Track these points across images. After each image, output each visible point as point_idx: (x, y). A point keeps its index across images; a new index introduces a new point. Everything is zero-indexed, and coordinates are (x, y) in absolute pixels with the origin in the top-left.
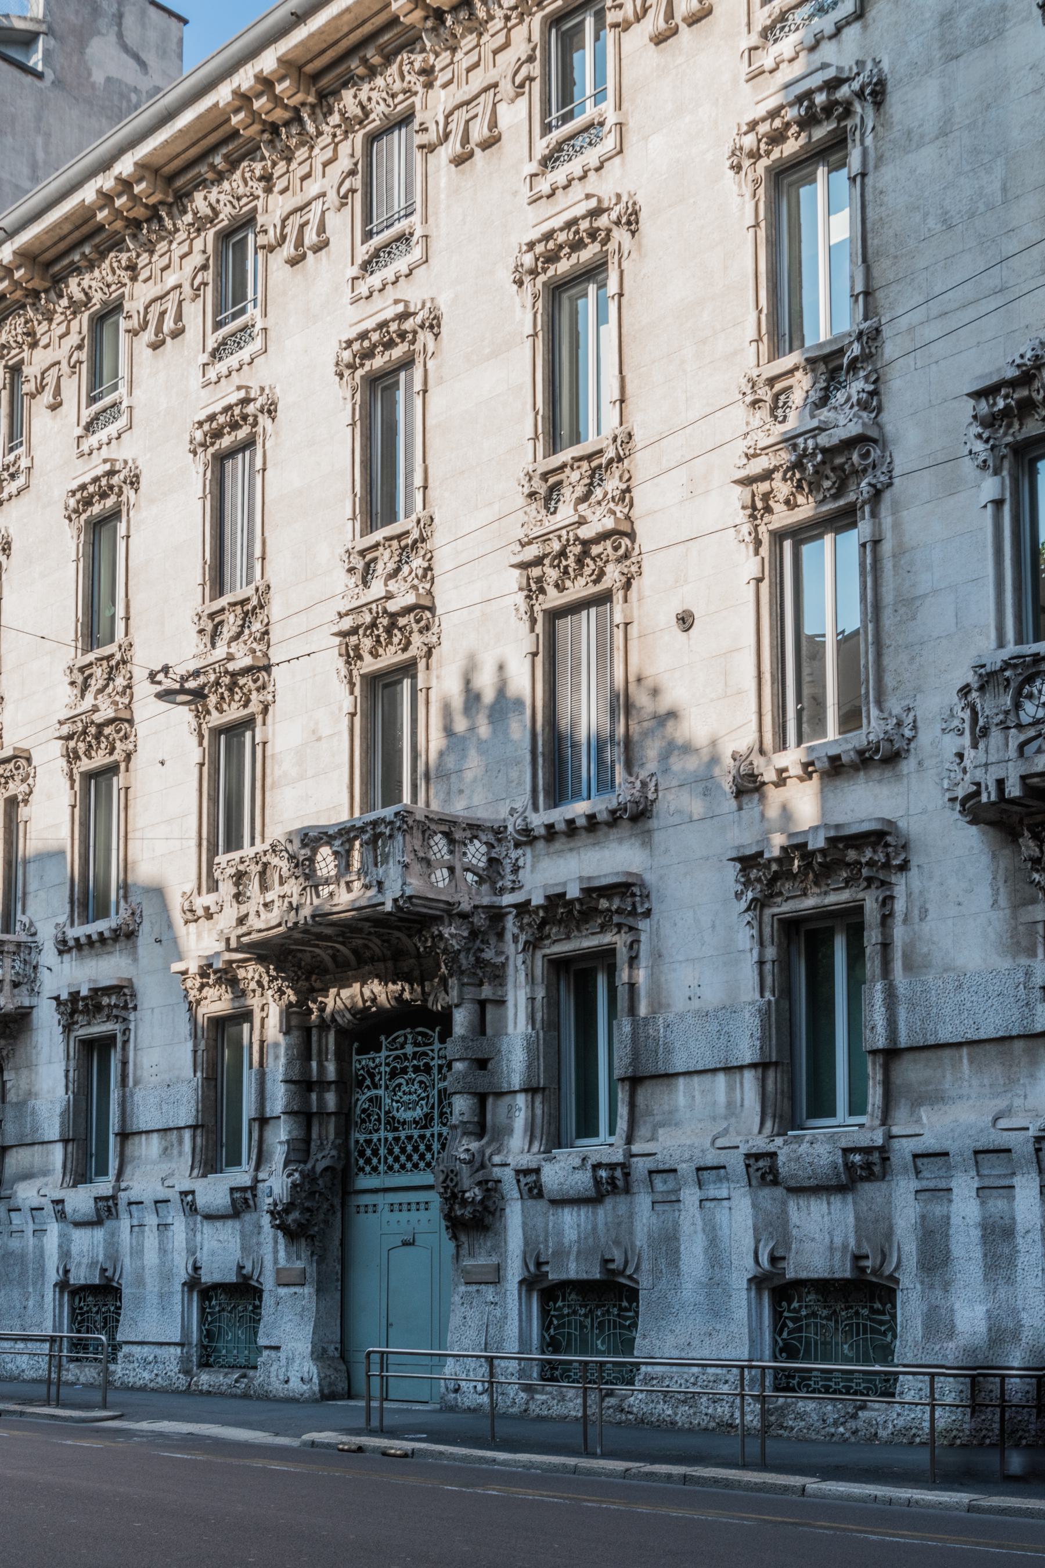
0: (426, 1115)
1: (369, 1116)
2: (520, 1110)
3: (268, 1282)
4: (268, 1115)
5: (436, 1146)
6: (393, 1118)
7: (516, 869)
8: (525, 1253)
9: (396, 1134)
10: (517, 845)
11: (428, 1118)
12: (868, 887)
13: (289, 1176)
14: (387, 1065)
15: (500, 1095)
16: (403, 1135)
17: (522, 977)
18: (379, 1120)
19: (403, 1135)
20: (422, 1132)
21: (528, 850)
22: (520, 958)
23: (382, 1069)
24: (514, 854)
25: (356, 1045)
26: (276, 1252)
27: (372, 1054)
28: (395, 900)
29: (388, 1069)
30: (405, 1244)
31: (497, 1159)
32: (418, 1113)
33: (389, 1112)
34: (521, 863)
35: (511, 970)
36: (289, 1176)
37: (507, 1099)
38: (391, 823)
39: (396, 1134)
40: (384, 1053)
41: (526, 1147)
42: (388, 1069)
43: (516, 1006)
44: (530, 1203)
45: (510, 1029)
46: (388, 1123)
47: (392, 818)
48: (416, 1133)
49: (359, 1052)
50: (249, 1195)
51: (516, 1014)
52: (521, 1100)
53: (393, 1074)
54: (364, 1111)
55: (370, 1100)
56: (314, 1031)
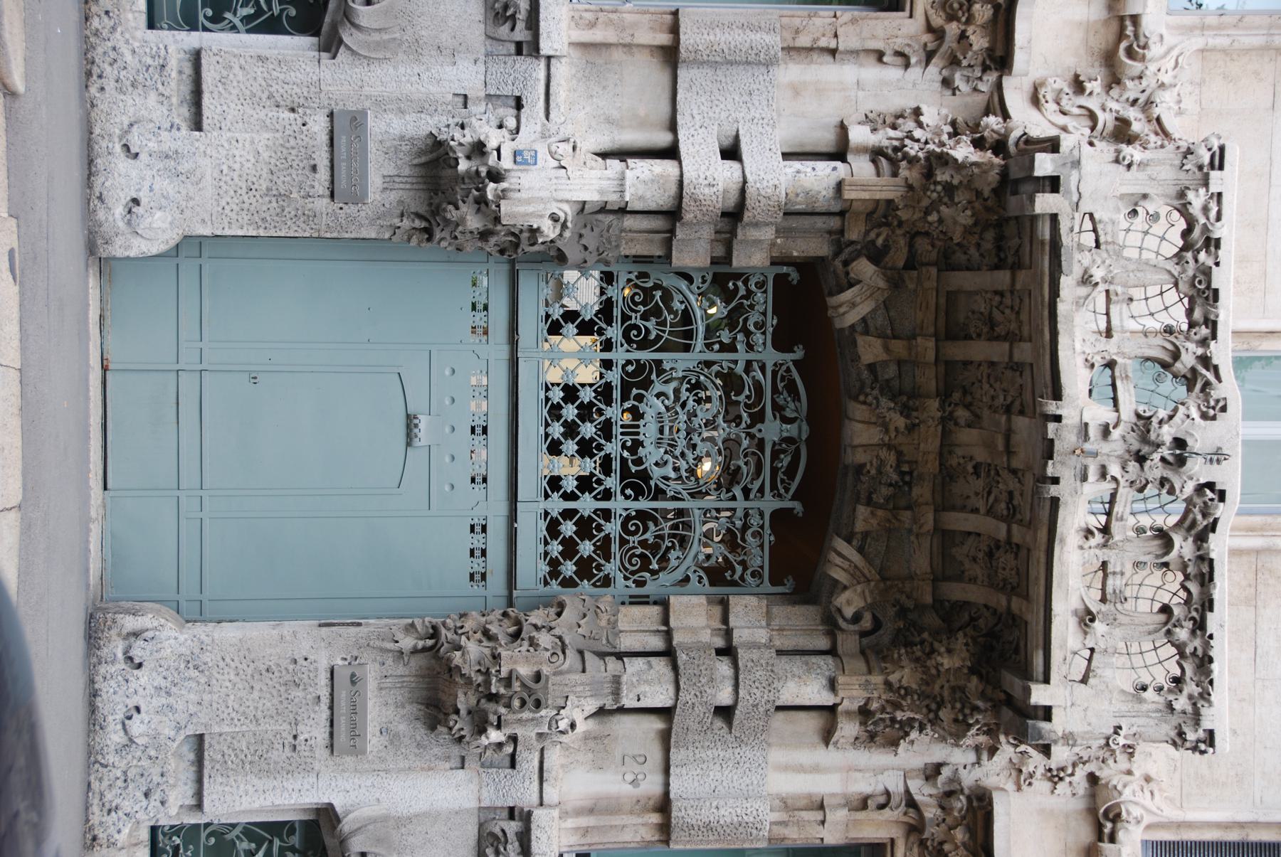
0: (645, 476)
1: (656, 312)
2: (634, 782)
3: (340, 79)
4: (682, 73)
5: (586, 505)
6: (647, 384)
7: (1055, 777)
8: (385, 819)
9: (617, 394)
10: (1093, 779)
11: (637, 483)
12: (930, 28)
13: (554, 218)
14: (749, 364)
15: (665, 738)
16: (613, 412)
17: (864, 785)
18: (644, 345)
19: (613, 412)
20: (616, 465)
21: (1079, 804)
22: (894, 784)
23: (742, 355)
24: (1081, 773)
25: (794, 276)
26: (401, 106)
27: (771, 321)
28: (1047, 713)
29: (740, 369)
30: (410, 422)
31: (554, 757)
32: (651, 453)
33: (660, 372)
34: (1061, 787)
35: (880, 757)
36: (554, 218)
37: (655, 754)
38: (1196, 717)
39: (617, 394)
40: (771, 356)
41: (569, 807)
42: (740, 369)
43: (816, 769)
44: (472, 831)
45: (777, 755)
46: (640, 367)
47: (1206, 724)
48: (613, 448)
49: (778, 278)
50: (521, 34)
51: (801, 769)
52: (651, 786)
53: (731, 382)
54: (667, 297)
55: (687, 317)
56: (834, 223)
